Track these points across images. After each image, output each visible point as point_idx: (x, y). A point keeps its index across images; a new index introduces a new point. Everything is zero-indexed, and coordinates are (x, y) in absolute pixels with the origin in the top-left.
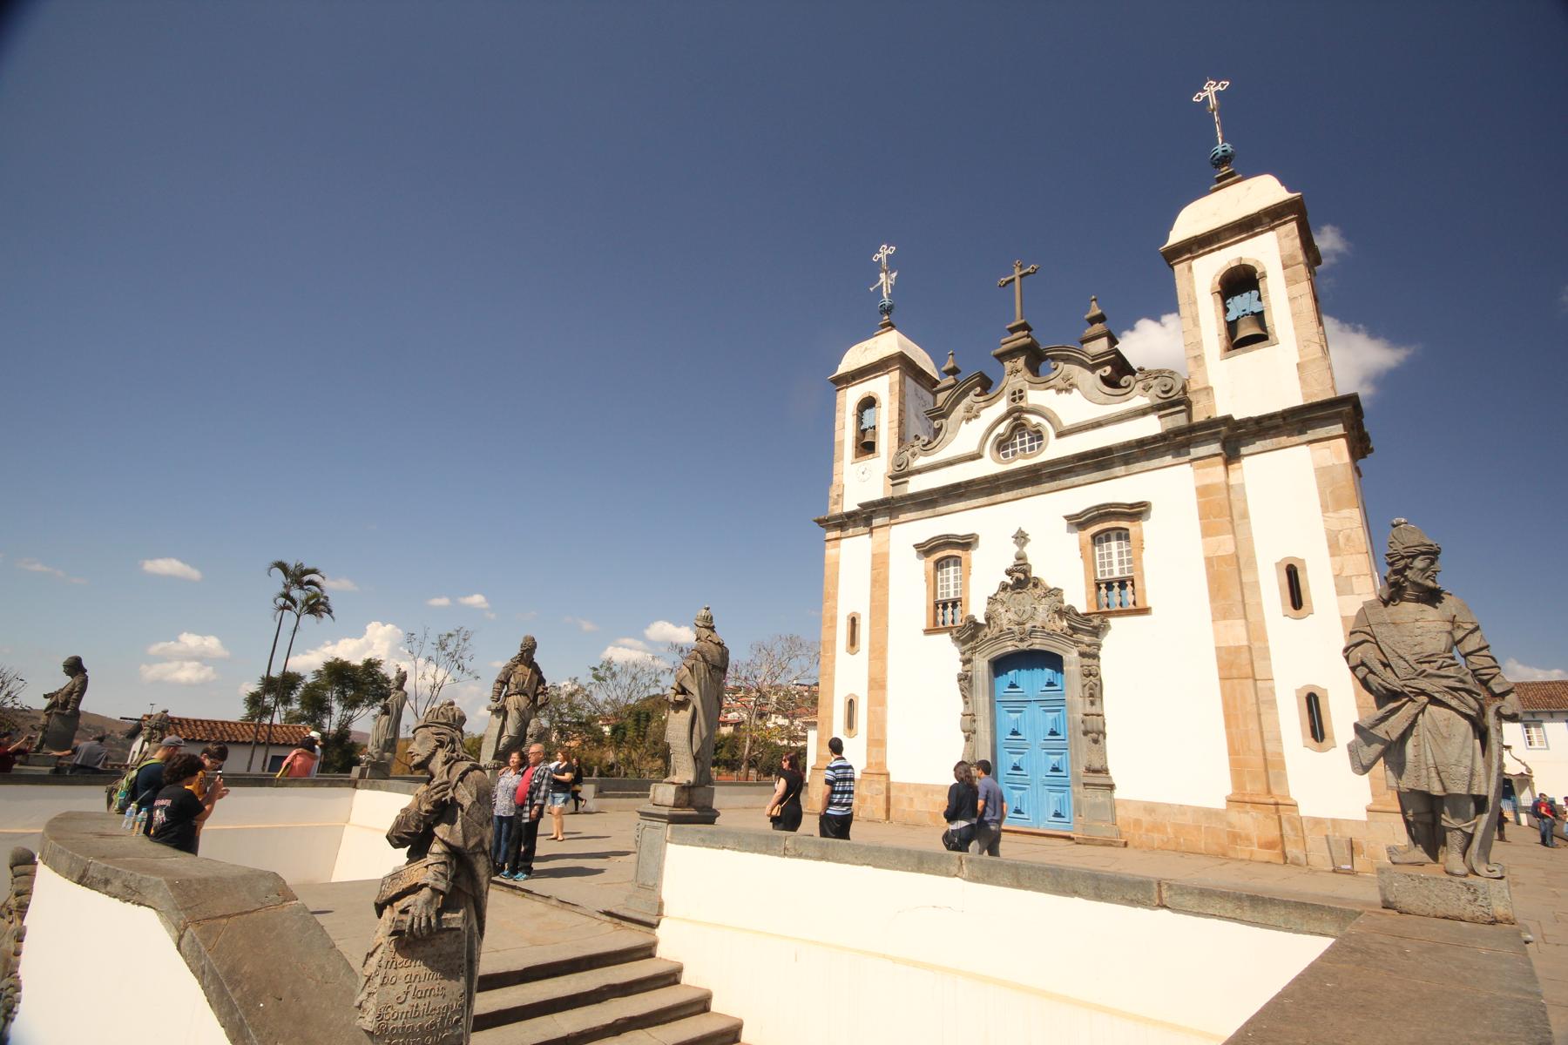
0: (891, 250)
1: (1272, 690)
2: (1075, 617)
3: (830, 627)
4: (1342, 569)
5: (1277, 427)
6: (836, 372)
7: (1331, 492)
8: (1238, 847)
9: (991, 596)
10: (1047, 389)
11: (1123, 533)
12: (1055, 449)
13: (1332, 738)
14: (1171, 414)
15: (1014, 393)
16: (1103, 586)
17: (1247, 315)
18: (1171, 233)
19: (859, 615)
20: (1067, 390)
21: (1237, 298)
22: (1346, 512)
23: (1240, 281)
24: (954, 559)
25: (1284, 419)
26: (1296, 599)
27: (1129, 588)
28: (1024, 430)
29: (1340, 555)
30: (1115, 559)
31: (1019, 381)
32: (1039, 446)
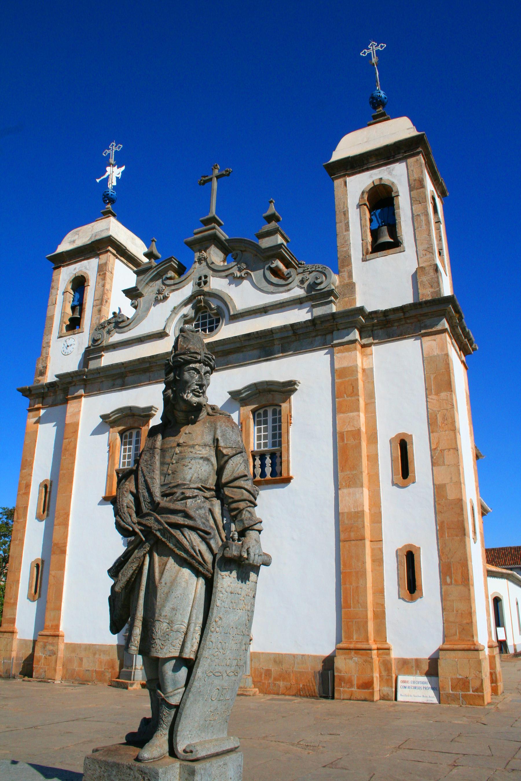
0: (119, 147)
4: (438, 443)
6: (55, 251)
7: (435, 378)
8: (341, 689)
13: (421, 590)
15: (200, 278)
18: (334, 153)
20: (241, 278)
22: (443, 395)
25: (404, 313)
28: (206, 312)
29: (437, 432)
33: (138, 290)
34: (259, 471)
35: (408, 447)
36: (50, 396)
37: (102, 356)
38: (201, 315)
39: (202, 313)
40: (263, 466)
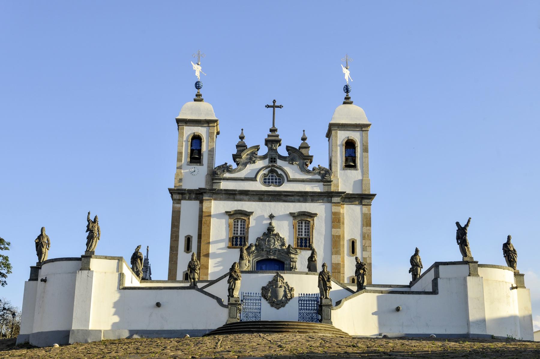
1: (344, 277)
2: (292, 249)
3: (175, 240)
5: (355, 198)
7: (366, 221)
9: (259, 237)
10: (285, 161)
11: (307, 222)
12: (286, 187)
14: (327, 185)
15: (272, 159)
16: (299, 239)
17: (351, 157)
19: (192, 237)
21: (349, 149)
22: (368, 228)
23: (350, 145)
24: (241, 220)
25: (358, 196)
26: (353, 251)
27: (308, 242)
29: (365, 240)
30: (303, 230)
31: (274, 154)
32: (279, 182)
33: (241, 156)
34: (299, 244)
35: (355, 243)
36: (186, 195)
37: (221, 182)
38: (271, 175)
39: (271, 174)
40: (301, 243)
